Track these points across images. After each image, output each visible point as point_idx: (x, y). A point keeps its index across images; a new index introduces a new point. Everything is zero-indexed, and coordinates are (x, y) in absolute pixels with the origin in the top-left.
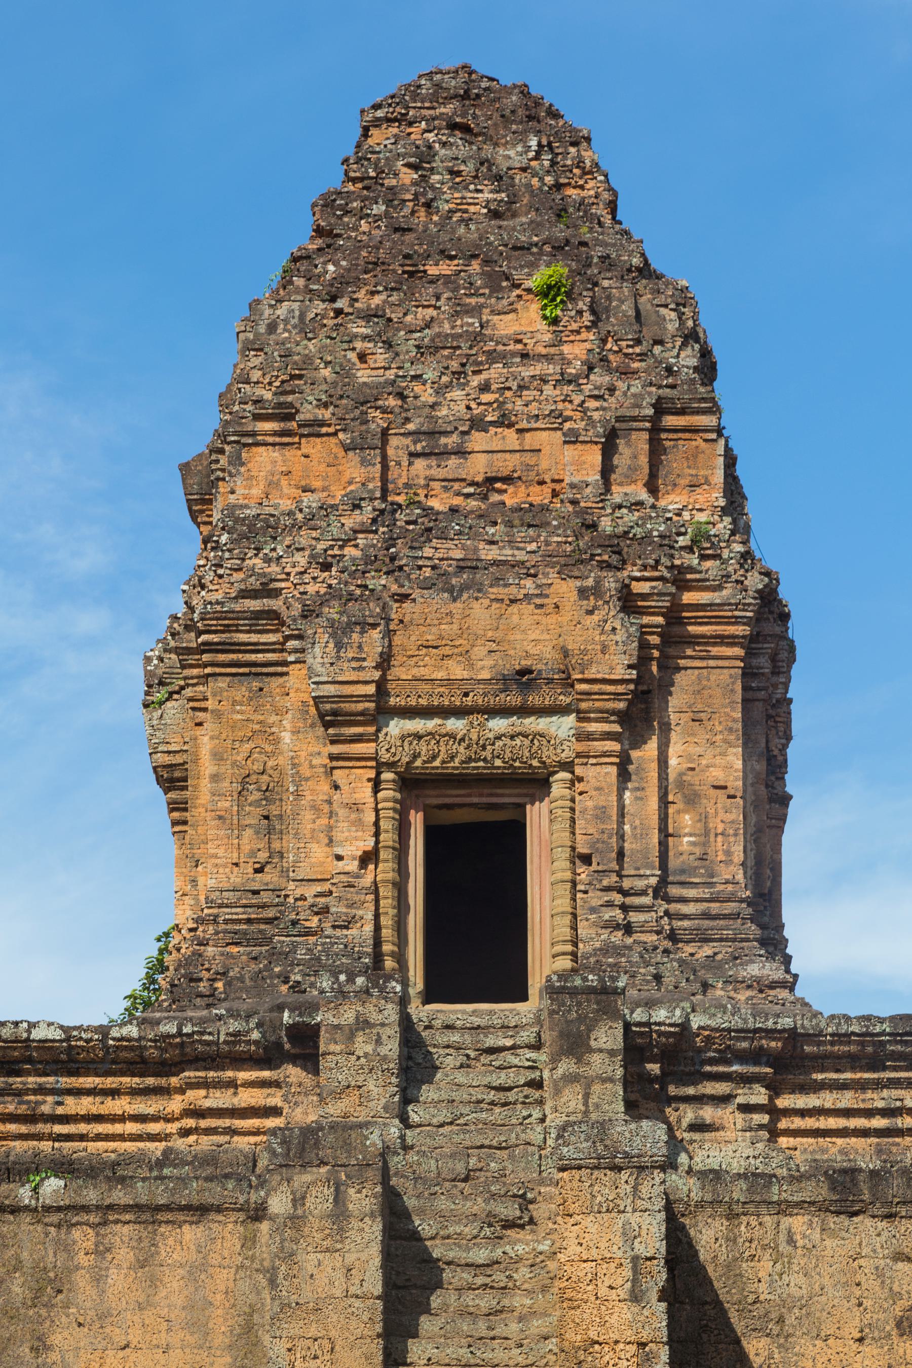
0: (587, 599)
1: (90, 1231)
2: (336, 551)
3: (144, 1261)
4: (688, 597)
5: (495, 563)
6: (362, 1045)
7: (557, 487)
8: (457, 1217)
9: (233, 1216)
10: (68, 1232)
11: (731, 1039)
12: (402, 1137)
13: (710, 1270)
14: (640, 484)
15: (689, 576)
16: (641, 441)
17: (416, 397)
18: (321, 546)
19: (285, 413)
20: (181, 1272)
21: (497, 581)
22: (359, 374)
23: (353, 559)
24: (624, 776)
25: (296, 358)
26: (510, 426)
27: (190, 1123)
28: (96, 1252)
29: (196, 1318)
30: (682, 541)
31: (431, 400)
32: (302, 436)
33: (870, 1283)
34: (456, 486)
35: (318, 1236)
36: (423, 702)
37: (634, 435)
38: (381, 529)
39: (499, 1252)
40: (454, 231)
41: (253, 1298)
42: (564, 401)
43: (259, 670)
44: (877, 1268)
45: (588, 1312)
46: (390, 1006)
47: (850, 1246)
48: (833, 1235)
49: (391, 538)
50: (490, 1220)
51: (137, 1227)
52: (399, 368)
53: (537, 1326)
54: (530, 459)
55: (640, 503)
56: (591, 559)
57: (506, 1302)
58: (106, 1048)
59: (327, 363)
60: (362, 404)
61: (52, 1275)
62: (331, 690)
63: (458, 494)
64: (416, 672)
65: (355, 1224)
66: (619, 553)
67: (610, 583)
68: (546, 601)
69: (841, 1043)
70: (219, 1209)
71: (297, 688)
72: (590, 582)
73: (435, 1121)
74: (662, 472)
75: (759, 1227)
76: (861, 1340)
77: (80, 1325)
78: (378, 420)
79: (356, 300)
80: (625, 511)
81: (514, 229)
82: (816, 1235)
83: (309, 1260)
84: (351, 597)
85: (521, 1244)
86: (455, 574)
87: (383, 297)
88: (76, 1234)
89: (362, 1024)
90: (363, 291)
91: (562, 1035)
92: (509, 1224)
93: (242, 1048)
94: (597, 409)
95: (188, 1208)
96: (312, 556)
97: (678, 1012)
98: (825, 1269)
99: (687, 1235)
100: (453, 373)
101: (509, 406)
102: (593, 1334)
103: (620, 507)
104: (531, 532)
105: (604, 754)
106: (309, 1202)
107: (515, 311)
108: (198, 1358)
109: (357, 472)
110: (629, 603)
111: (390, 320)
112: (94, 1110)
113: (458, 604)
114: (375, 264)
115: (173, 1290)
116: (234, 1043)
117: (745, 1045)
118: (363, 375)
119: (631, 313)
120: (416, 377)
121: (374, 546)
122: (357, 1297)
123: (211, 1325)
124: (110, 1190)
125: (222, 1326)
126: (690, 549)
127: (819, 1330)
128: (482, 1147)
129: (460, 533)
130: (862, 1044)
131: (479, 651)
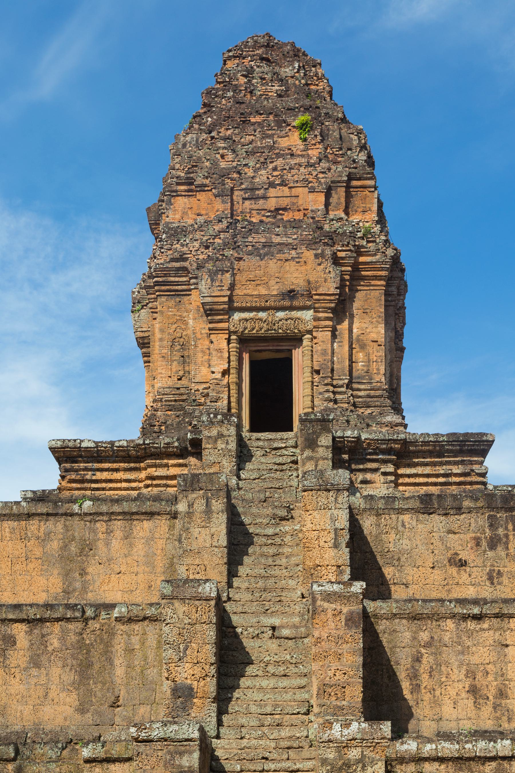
0: (318, 258)
1: (104, 523)
2: (211, 241)
4: (362, 259)
5: (279, 244)
6: (220, 445)
7: (306, 212)
8: (260, 516)
9: (165, 517)
10: (95, 524)
11: (378, 444)
12: (238, 484)
13: (369, 538)
14: (341, 210)
15: (362, 250)
16: (342, 191)
17: (245, 174)
18: (205, 238)
19: (189, 182)
20: (143, 541)
21: (280, 251)
22: (221, 164)
23: (219, 244)
24: (334, 336)
25: (194, 158)
26: (286, 185)
27: (149, 482)
28: (107, 533)
29: (149, 561)
30: (359, 235)
31: (252, 175)
32: (197, 191)
33: (437, 543)
34: (263, 212)
35: (199, 521)
36: (248, 305)
37: (339, 189)
38: (231, 231)
39: (278, 530)
40: (262, 103)
41: (173, 551)
42: (309, 174)
43: (179, 293)
44: (440, 537)
45: (316, 553)
46: (232, 428)
47: (429, 527)
48: (422, 522)
49: (235, 235)
50: (274, 517)
51: (124, 522)
52: (238, 161)
53: (294, 560)
54: (294, 200)
55: (341, 219)
56: (320, 242)
57: (280, 550)
58: (113, 450)
59: (208, 160)
60: (222, 177)
61: (88, 542)
62: (209, 300)
63: (264, 216)
64: (245, 292)
65: (215, 515)
66: (332, 239)
67: (328, 252)
68: (301, 260)
69: (425, 446)
70: (159, 514)
71: (195, 299)
72: (319, 251)
73: (251, 478)
74: (351, 206)
75: (390, 520)
76: (433, 568)
77: (100, 564)
78: (229, 184)
79: (220, 132)
80: (335, 222)
81: (288, 101)
82: (414, 523)
83: (195, 531)
84: (217, 259)
85: (287, 527)
86: (262, 249)
87: (232, 131)
88: (98, 525)
89: (221, 435)
90: (223, 129)
91: (306, 439)
92: (283, 519)
93: (171, 450)
94: (323, 178)
95: (145, 513)
96: (201, 243)
97: (356, 432)
98: (418, 537)
99: (359, 523)
100: (261, 163)
101: (285, 177)
102: (317, 562)
103: (333, 220)
104: (294, 230)
105: (326, 327)
106: (195, 506)
107: (288, 136)
108: (150, 577)
109: (220, 206)
110: (336, 261)
111: (234, 141)
112: (109, 478)
113: (263, 262)
114: (228, 117)
115: (139, 549)
116: (167, 448)
117: (384, 446)
118: (223, 164)
119: (338, 136)
120: (246, 165)
121: (227, 238)
122: (216, 547)
123: (155, 563)
124: (112, 506)
125: (160, 564)
126: (362, 238)
127: (415, 563)
128: (272, 488)
129: (264, 231)
130: (434, 446)
131: (272, 282)
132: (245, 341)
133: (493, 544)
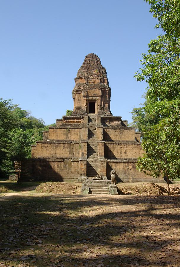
3: (74, 131)
132: (88, 100)
133: (121, 134)
